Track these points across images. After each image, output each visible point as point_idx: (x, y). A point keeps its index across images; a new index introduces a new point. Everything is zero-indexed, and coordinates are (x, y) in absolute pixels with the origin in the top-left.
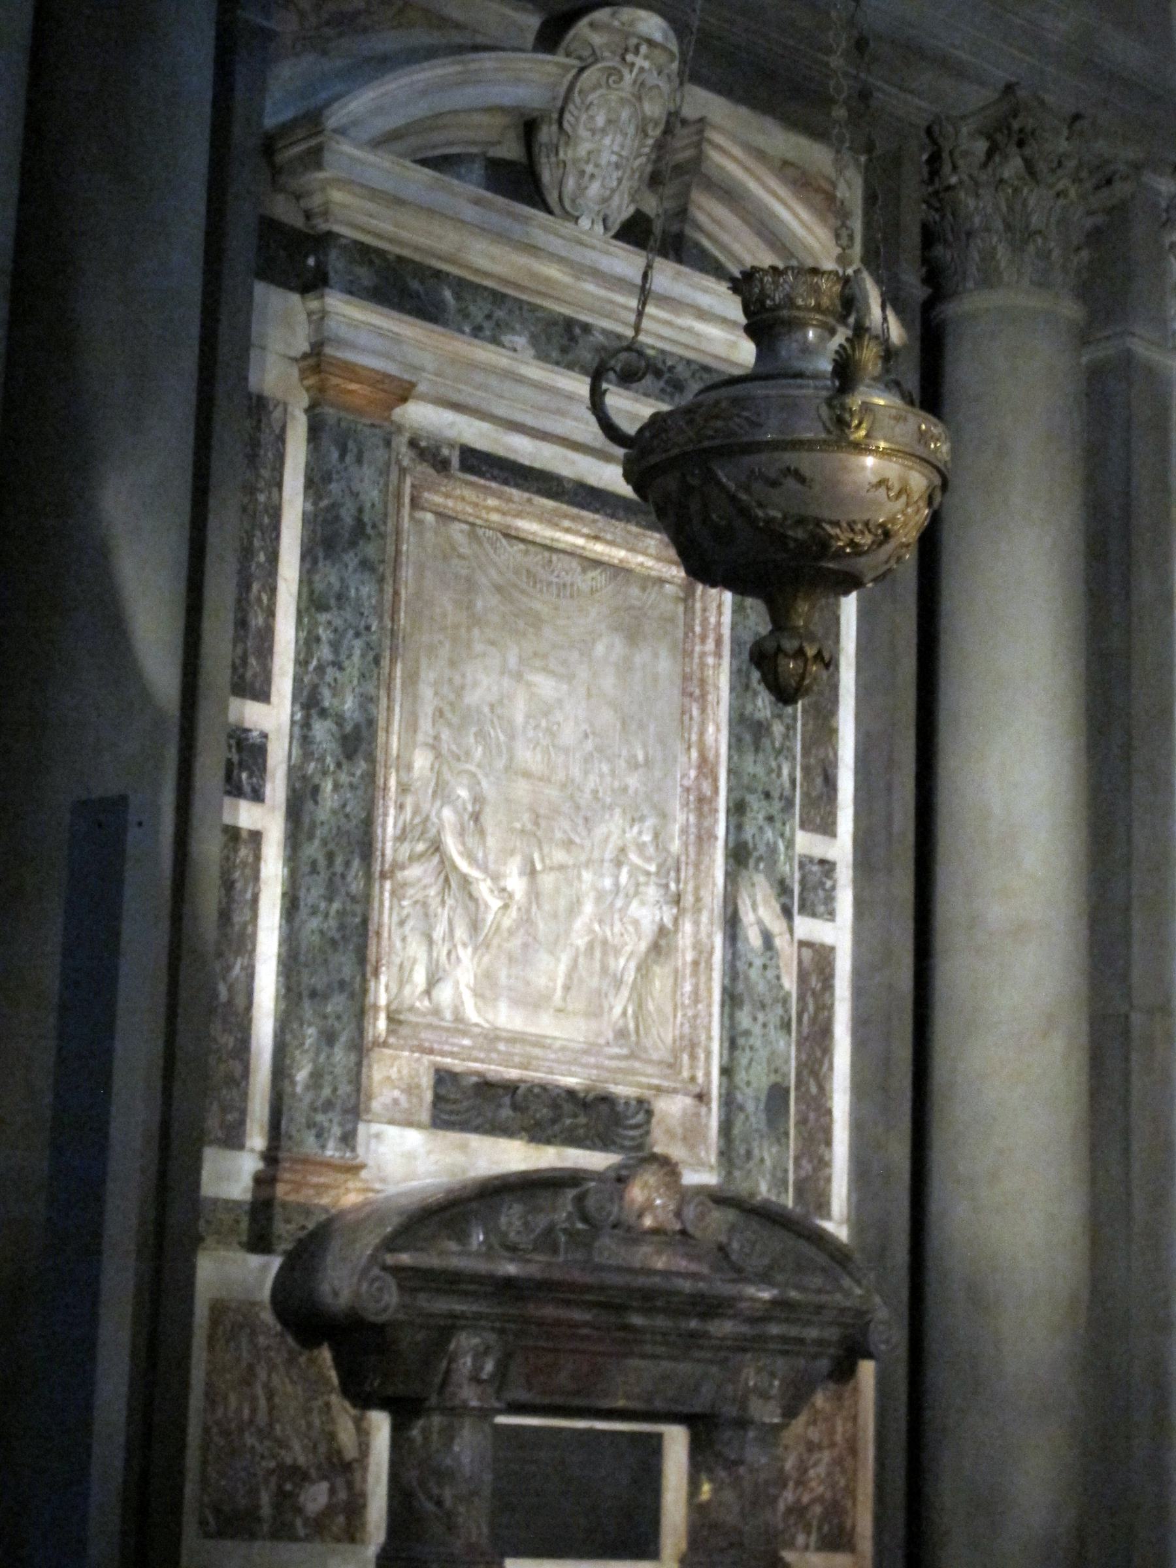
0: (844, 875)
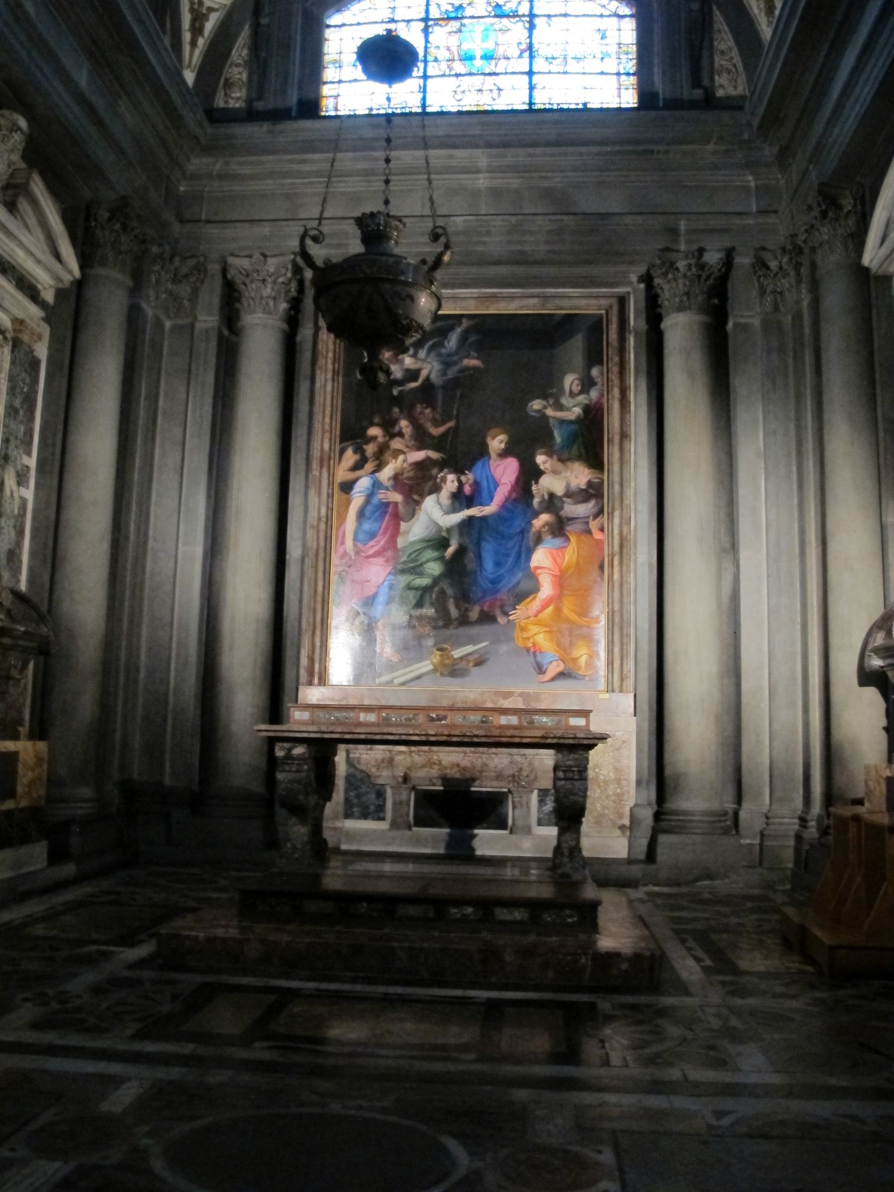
0: (33, 473)
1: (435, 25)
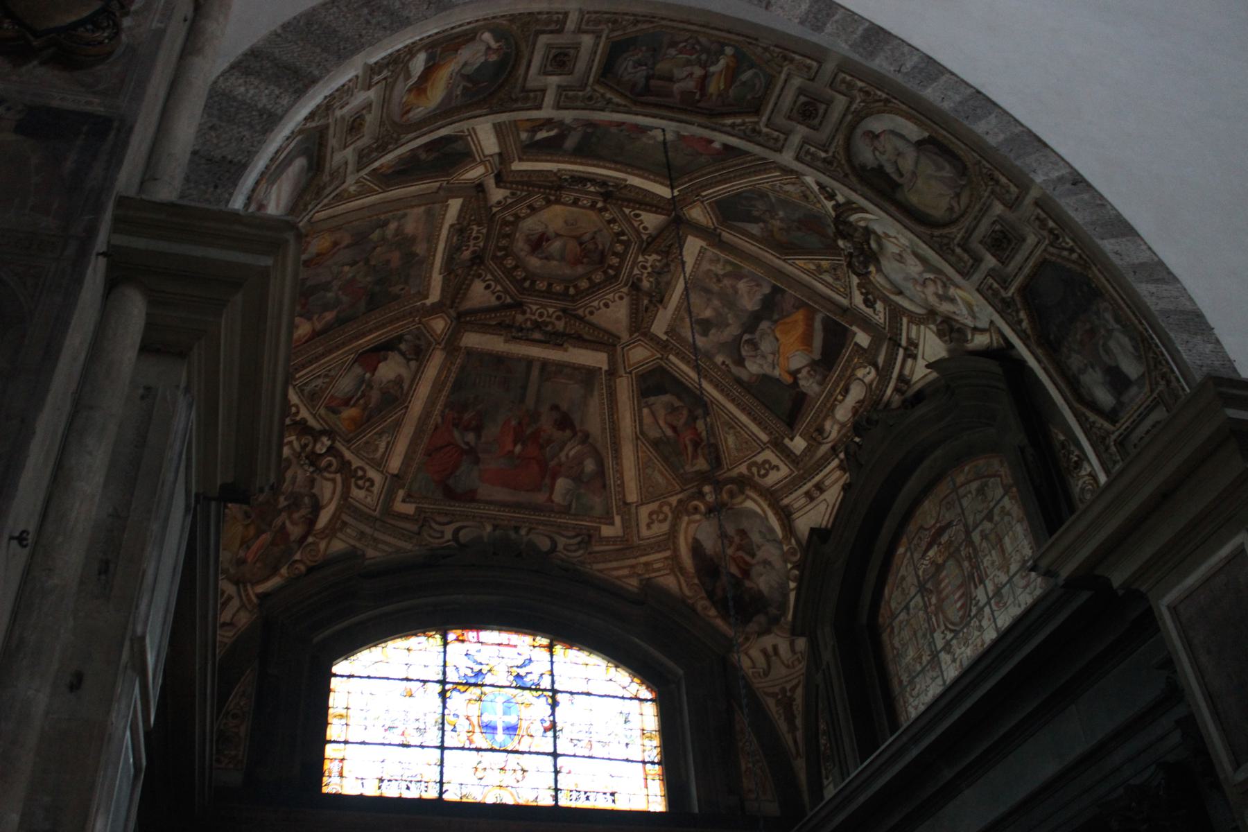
1: (454, 689)
